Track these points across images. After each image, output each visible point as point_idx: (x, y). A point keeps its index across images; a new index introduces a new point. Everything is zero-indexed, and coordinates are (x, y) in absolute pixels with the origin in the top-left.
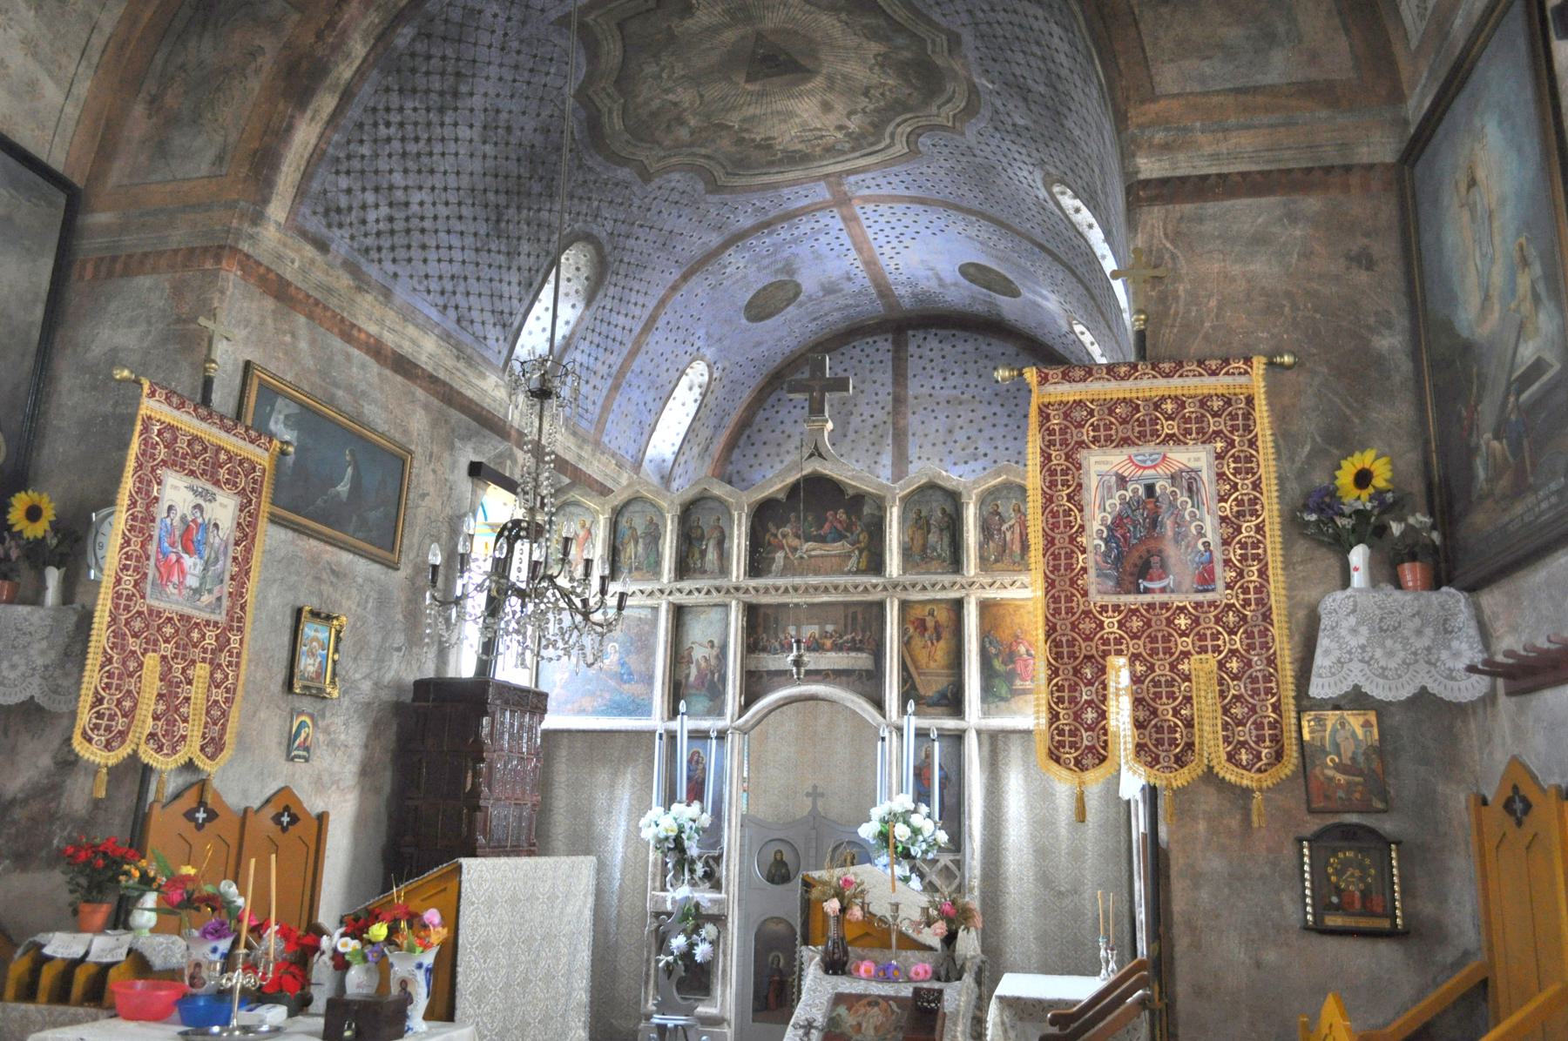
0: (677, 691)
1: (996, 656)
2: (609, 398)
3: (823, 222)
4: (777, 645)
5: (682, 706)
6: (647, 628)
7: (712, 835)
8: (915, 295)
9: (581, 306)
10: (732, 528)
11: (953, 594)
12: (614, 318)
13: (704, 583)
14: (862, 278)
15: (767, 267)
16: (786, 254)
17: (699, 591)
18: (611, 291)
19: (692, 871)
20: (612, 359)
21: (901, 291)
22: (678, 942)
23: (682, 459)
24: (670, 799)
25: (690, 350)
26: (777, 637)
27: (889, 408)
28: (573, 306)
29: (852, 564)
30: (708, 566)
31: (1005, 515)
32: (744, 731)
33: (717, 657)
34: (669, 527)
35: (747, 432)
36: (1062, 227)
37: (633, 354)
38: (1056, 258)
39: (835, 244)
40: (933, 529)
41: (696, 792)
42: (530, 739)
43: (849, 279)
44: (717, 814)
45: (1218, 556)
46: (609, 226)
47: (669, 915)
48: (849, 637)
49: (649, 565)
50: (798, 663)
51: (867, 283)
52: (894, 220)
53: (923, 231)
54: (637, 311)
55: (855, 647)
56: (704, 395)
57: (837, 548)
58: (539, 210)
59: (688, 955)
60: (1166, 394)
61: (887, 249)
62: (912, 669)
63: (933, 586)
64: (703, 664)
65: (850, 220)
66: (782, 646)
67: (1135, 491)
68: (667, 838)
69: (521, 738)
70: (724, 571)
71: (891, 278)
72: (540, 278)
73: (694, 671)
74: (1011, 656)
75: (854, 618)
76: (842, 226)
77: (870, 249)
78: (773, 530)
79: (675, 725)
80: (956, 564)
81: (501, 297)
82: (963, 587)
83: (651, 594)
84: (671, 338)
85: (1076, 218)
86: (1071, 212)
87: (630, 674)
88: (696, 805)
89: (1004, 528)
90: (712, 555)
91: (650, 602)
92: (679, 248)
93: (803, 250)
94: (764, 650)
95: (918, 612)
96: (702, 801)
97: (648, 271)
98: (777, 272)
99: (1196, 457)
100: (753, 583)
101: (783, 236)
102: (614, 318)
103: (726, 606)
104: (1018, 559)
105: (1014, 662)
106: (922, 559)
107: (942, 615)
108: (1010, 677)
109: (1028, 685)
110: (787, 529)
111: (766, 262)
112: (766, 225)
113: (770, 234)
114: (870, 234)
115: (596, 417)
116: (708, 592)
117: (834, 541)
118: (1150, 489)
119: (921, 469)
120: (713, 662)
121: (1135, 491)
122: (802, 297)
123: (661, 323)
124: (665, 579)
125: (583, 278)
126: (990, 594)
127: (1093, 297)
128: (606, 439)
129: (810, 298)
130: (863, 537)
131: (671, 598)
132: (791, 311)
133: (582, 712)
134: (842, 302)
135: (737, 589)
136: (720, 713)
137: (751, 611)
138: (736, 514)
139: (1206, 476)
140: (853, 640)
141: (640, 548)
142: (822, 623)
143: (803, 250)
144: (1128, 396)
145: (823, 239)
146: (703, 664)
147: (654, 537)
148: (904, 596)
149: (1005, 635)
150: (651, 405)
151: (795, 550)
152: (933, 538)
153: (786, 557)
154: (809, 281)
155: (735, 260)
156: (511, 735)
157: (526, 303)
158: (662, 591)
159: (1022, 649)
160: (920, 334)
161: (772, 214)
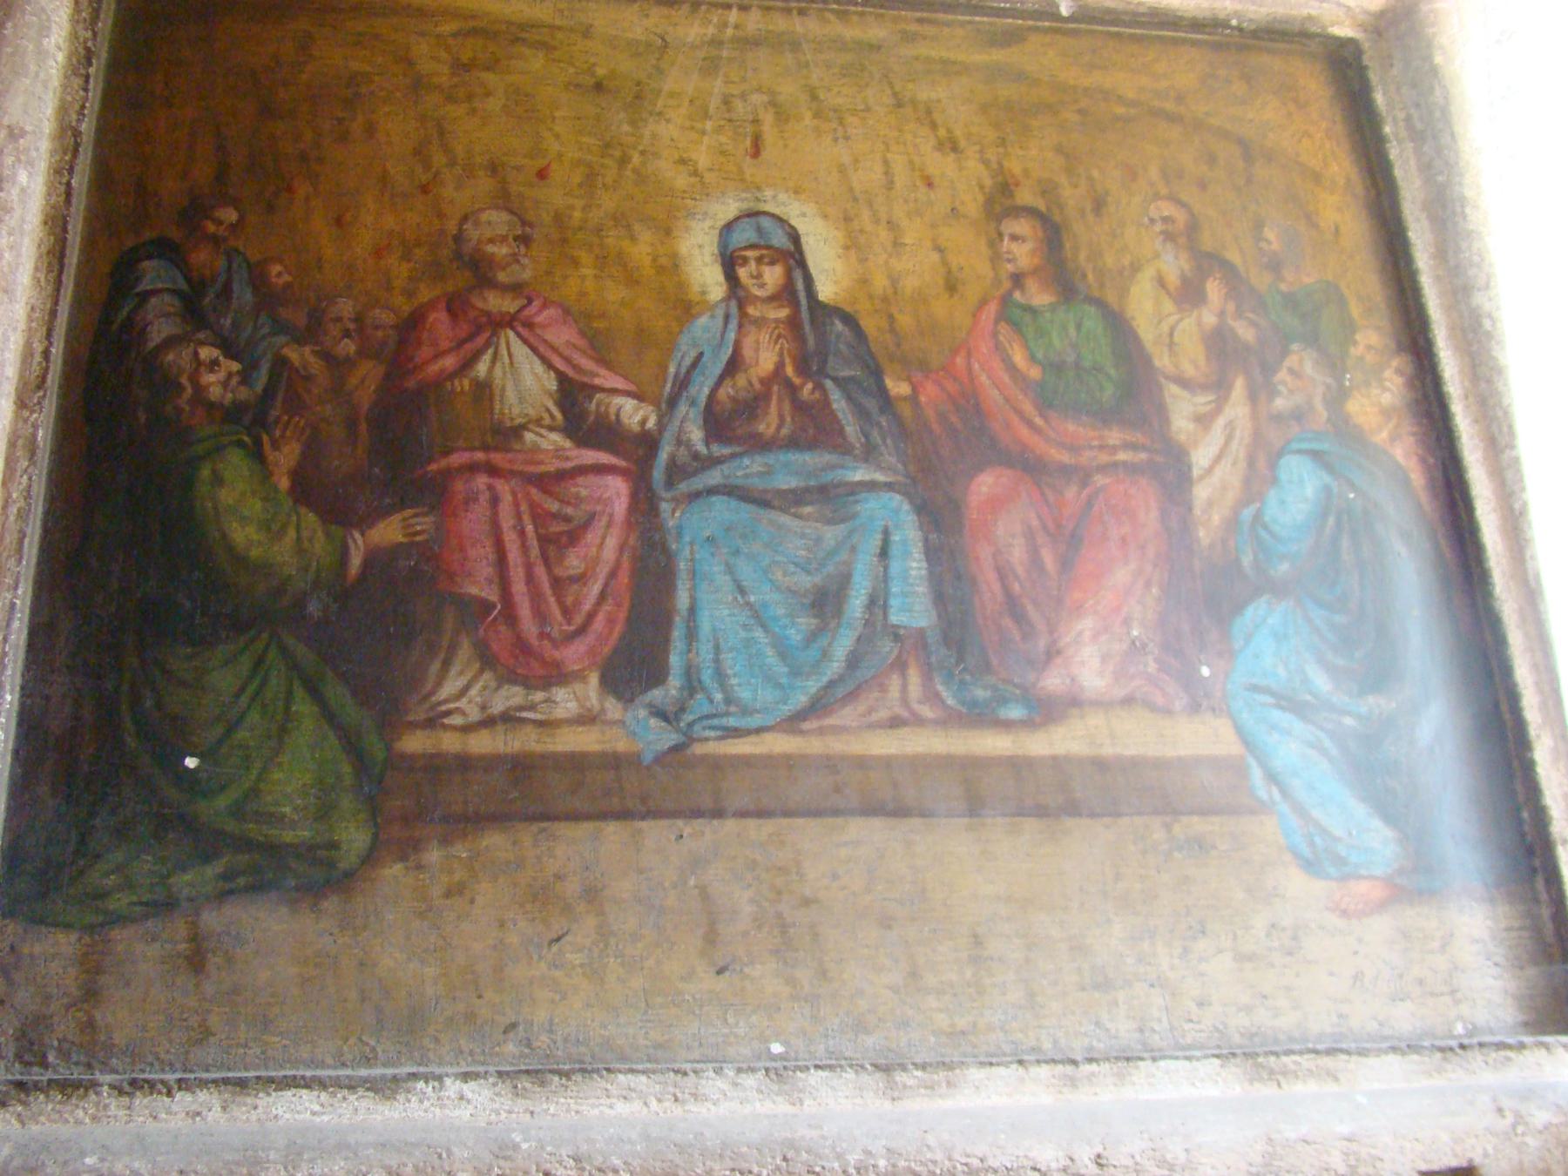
74: (406, 438)
105: (434, 494)
108: (375, 632)
109: (578, 716)
149: (355, 245)
159: (522, 380)
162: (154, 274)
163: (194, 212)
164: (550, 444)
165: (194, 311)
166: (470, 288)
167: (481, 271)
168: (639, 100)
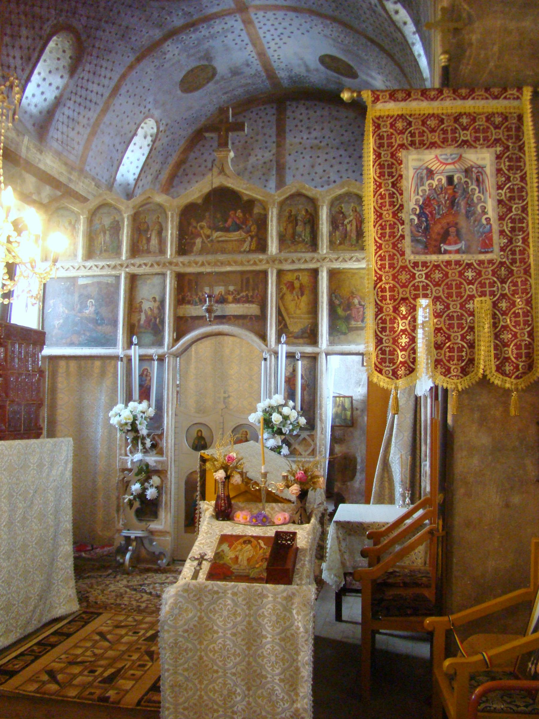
0: (132, 329)
1: (339, 305)
2: (89, 141)
3: (229, 25)
4: (197, 299)
5: (135, 339)
6: (112, 289)
7: (156, 421)
8: (290, 78)
9: (66, 77)
10: (167, 222)
11: (312, 266)
12: (90, 86)
13: (148, 260)
14: (257, 65)
16: (206, 46)
17: (146, 265)
18: (88, 67)
19: (143, 444)
20: (90, 114)
21: (282, 74)
22: (136, 487)
23: (140, 184)
24: (129, 398)
25: (143, 110)
26: (197, 295)
27: (274, 151)
28: (62, 77)
29: (246, 246)
30: (152, 248)
31: (347, 214)
32: (177, 355)
33: (158, 308)
35: (183, 167)
36: (386, 24)
37: (104, 111)
38: (382, 49)
39: (238, 40)
40: (299, 223)
41: (145, 394)
42: (34, 362)
43: (248, 65)
44: (159, 408)
45: (495, 228)
46: (84, 20)
47: (130, 470)
48: (244, 294)
50: (209, 311)
51: (260, 68)
52: (276, 23)
53: (295, 31)
54: (106, 82)
55: (248, 300)
56: (154, 142)
57: (235, 236)
58: (33, 6)
59: (141, 496)
60: (463, 111)
61: (272, 44)
62: (285, 314)
63: (299, 260)
64: (149, 313)
65: (248, 22)
66: (200, 300)
67: (440, 180)
68: (126, 424)
69: (28, 361)
70: (162, 251)
71: (275, 65)
72: (36, 55)
73: (143, 317)
74: (349, 306)
75: (248, 280)
76: (242, 27)
77: (261, 44)
78: (195, 224)
79: (128, 352)
80: (314, 245)
81: (9, 67)
82: (318, 261)
83: (115, 267)
84: (131, 101)
85: (396, 18)
86: (392, 13)
87: (102, 319)
88: (145, 404)
89: (345, 222)
90: (154, 241)
91: (113, 273)
92: (133, 39)
93: (216, 44)
94: (189, 303)
95: (289, 277)
96: (148, 400)
97: (113, 54)
98: (200, 59)
99: (483, 158)
100: (181, 259)
101: (203, 33)
102: (90, 86)
103: (164, 275)
104: (354, 242)
105: (351, 310)
106: (293, 243)
107: (305, 279)
108: (348, 319)
109: (359, 324)
110: (204, 224)
111: (192, 51)
112: (192, 25)
113: (195, 31)
114: (261, 32)
115: (80, 153)
116: (152, 265)
117: (235, 231)
118: (450, 179)
119: (293, 185)
120: (156, 311)
121: (440, 180)
122: (217, 77)
123: (123, 90)
124: (124, 258)
125: (68, 58)
126: (336, 265)
127: (405, 75)
128: (87, 168)
129: (222, 78)
130: (254, 228)
131: (127, 270)
132: (211, 86)
133: (72, 344)
134: (243, 81)
135: (171, 263)
136: (160, 344)
137: (180, 277)
138: (170, 214)
139: (490, 170)
140: (247, 295)
142: (226, 285)
143: (216, 44)
144: (436, 112)
145: (230, 36)
146: (149, 313)
148: (281, 267)
149: (345, 292)
150: (118, 147)
151: (208, 237)
152: (299, 229)
153: (203, 242)
154: (222, 66)
155: (172, 50)
156: (20, 359)
157: (27, 72)
158: (121, 265)
159: (356, 301)
160: (294, 104)
161: (195, 17)
162: (333, 295)
163: (335, 290)
164: (358, 306)
165: (336, 297)
166: (353, 295)
167: (353, 293)
168: (364, 278)
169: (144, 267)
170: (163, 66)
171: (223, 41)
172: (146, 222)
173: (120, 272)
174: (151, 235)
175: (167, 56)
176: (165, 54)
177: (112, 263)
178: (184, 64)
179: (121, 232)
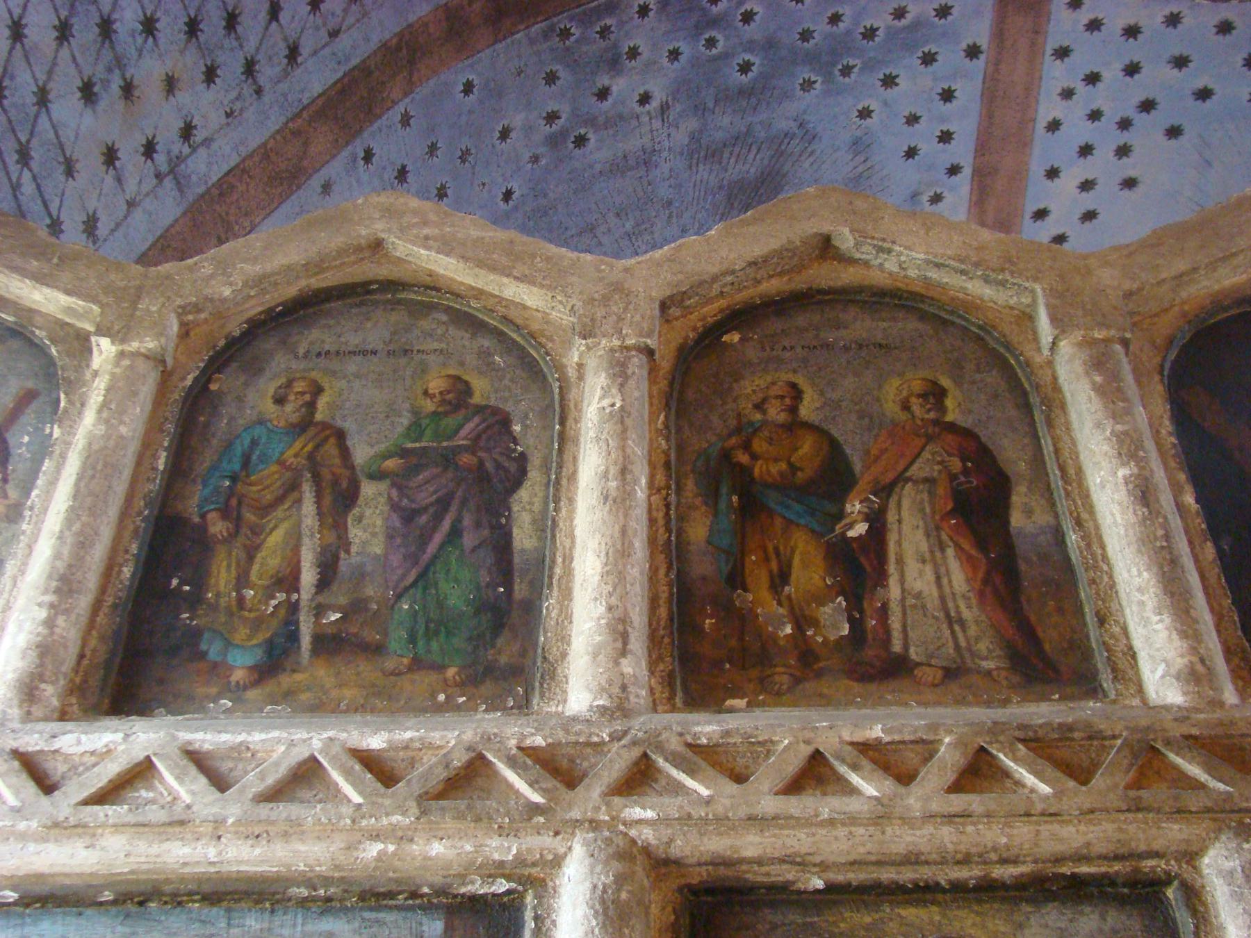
15: (713, 155)
16: (782, 118)
30: (916, 636)
34: (596, 402)
49: (435, 624)
83: (466, 781)
111: (725, 122)
114: (1056, 75)
116: (978, 772)
124: (580, 688)
141: (370, 529)
147: (478, 475)
169: (868, 786)
170: (581, 141)
171: (865, 113)
172: (795, 426)
173: (538, 842)
174: (877, 521)
175: (623, 86)
176: (613, 64)
177: (447, 737)
178: (664, 192)
179: (526, 500)
